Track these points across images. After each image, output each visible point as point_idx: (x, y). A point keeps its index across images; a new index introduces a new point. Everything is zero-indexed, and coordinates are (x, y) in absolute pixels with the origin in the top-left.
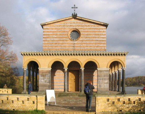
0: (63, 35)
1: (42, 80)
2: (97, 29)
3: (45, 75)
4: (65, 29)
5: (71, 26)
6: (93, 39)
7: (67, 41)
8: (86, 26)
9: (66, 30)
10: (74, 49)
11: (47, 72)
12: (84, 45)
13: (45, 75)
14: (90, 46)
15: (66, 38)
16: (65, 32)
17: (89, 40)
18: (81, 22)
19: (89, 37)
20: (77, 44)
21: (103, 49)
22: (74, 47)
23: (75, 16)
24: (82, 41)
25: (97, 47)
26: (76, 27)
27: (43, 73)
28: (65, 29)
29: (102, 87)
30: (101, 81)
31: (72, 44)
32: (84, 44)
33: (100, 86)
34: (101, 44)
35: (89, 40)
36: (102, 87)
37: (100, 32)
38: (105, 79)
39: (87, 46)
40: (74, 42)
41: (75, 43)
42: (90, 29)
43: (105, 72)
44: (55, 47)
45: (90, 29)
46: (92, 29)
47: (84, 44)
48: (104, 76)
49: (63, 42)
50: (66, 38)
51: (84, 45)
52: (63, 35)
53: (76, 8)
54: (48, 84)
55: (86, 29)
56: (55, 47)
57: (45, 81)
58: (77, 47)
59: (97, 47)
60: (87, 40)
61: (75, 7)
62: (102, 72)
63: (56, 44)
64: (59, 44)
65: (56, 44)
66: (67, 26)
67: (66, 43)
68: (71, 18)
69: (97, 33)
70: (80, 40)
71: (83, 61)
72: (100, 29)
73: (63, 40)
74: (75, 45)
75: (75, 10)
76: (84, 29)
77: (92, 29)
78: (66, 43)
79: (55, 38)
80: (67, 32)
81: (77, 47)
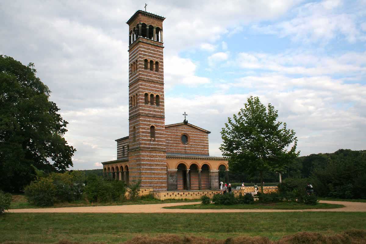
0: (177, 138)
1: (171, 180)
2: (202, 135)
3: (173, 175)
4: (177, 133)
5: (182, 131)
6: (200, 144)
7: (179, 144)
8: (194, 132)
9: (178, 134)
10: (186, 152)
11: (174, 172)
12: (192, 149)
13: (173, 175)
14: (198, 150)
15: (179, 141)
16: (177, 135)
17: (196, 145)
18: (190, 128)
19: (196, 142)
20: (188, 147)
21: (207, 153)
22: (185, 150)
23: (186, 123)
24: (191, 145)
25: (203, 151)
26: (187, 132)
27: (171, 173)
28: (177, 133)
29: (214, 185)
30: (213, 180)
31: (184, 147)
32: (193, 147)
33: (213, 184)
34: (205, 149)
35: (196, 145)
36: (214, 185)
37: (204, 138)
38: (216, 179)
39: (195, 150)
40: (186, 146)
41: (186, 147)
42: (197, 135)
43: (215, 173)
44: (171, 149)
45: (197, 135)
46: (199, 135)
47: (193, 147)
48: (215, 177)
49: (177, 145)
50: (179, 141)
51: (192, 149)
52: (177, 138)
53: (185, 113)
54: (176, 183)
55: (194, 134)
56: (171, 149)
57: (174, 181)
58: (188, 150)
59: (203, 151)
60: (195, 145)
61: (185, 114)
62: (214, 173)
63: (171, 146)
64: (173, 146)
65: (171, 146)
66: (180, 131)
67: (178, 146)
68: (183, 124)
69: (202, 139)
70: (190, 144)
71: (200, 164)
72: (204, 135)
73: (176, 143)
74: (186, 148)
75: (185, 117)
76: (192, 135)
77: (199, 135)
78: (179, 146)
79: (171, 140)
80: (179, 136)
81: (188, 150)
